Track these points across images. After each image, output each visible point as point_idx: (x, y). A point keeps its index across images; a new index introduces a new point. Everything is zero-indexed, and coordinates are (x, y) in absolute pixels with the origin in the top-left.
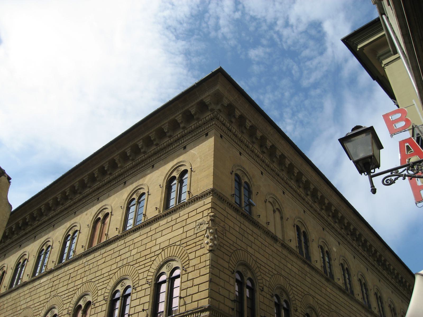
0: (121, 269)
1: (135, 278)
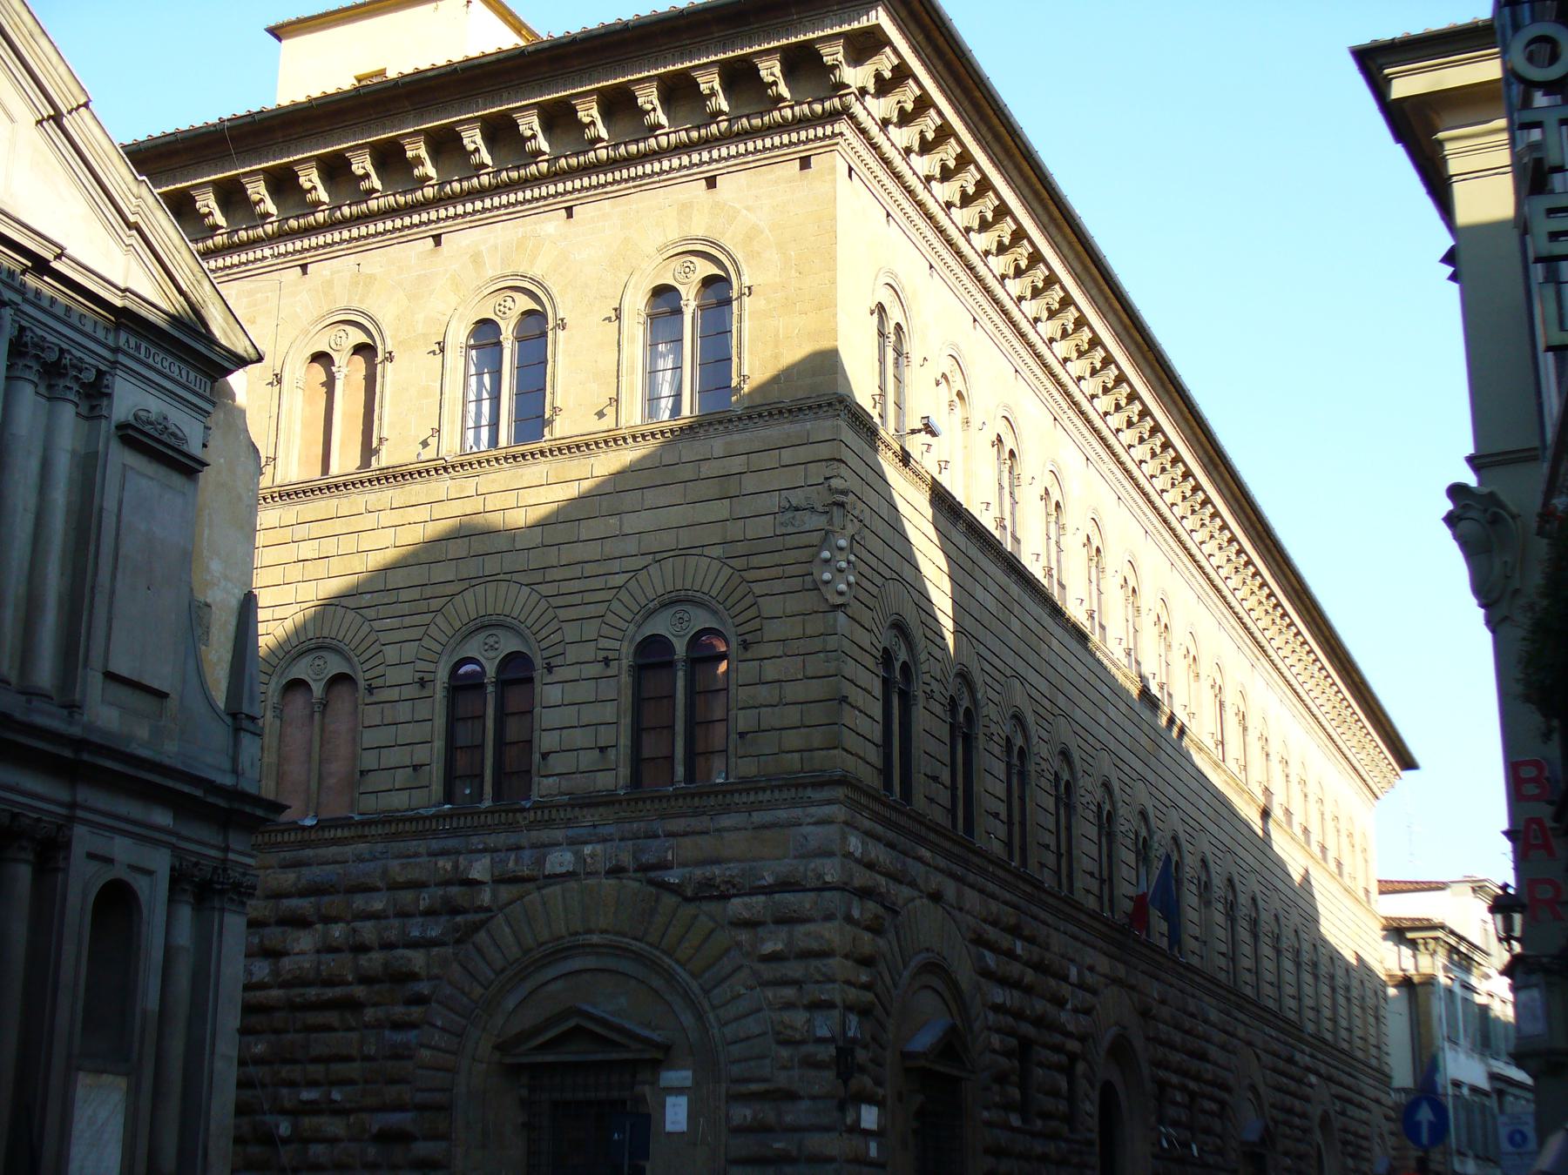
1: (544, 633)
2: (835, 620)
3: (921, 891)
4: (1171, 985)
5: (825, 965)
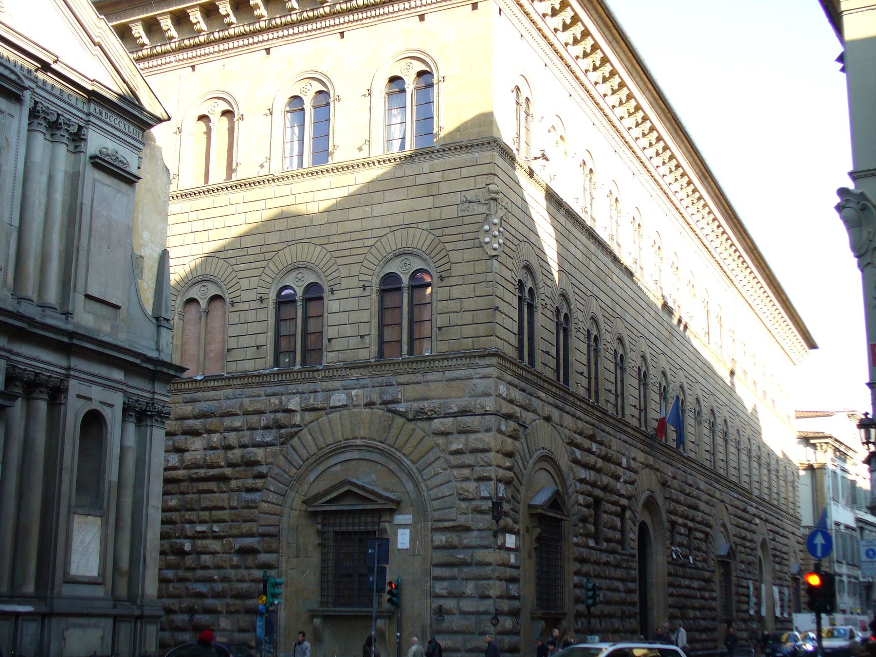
1: (329, 272)
2: (492, 265)
4: (679, 469)
5: (486, 457)
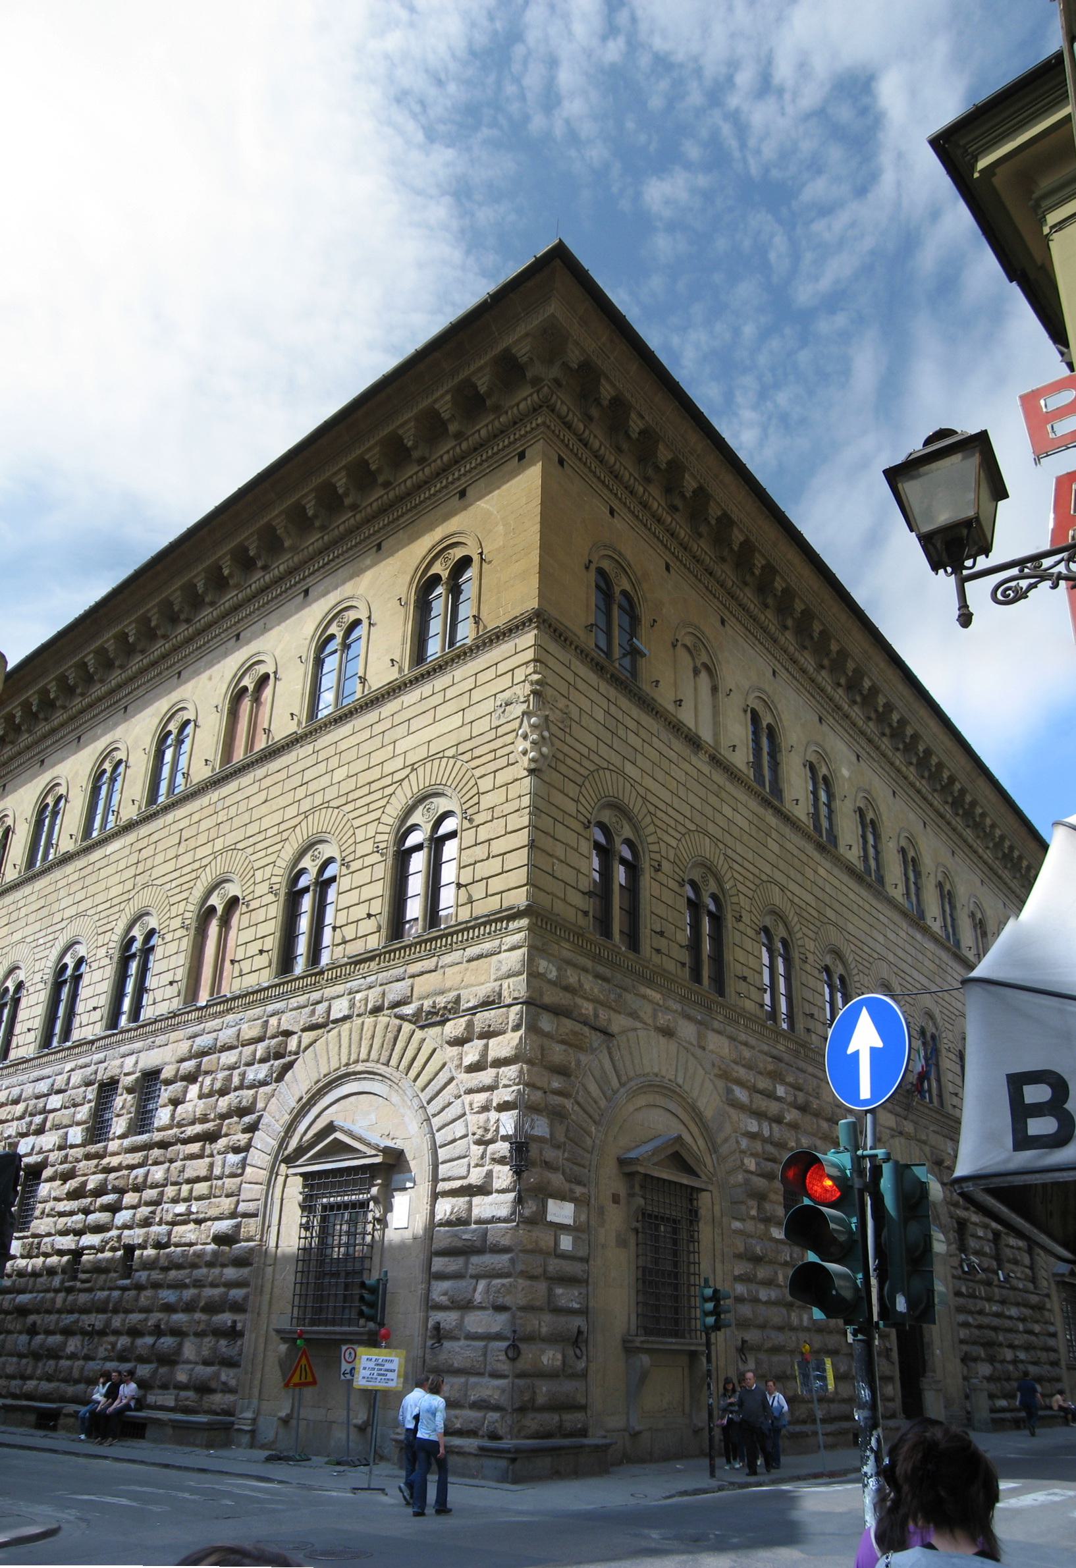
0: (310, 818)
3: (645, 1023)
